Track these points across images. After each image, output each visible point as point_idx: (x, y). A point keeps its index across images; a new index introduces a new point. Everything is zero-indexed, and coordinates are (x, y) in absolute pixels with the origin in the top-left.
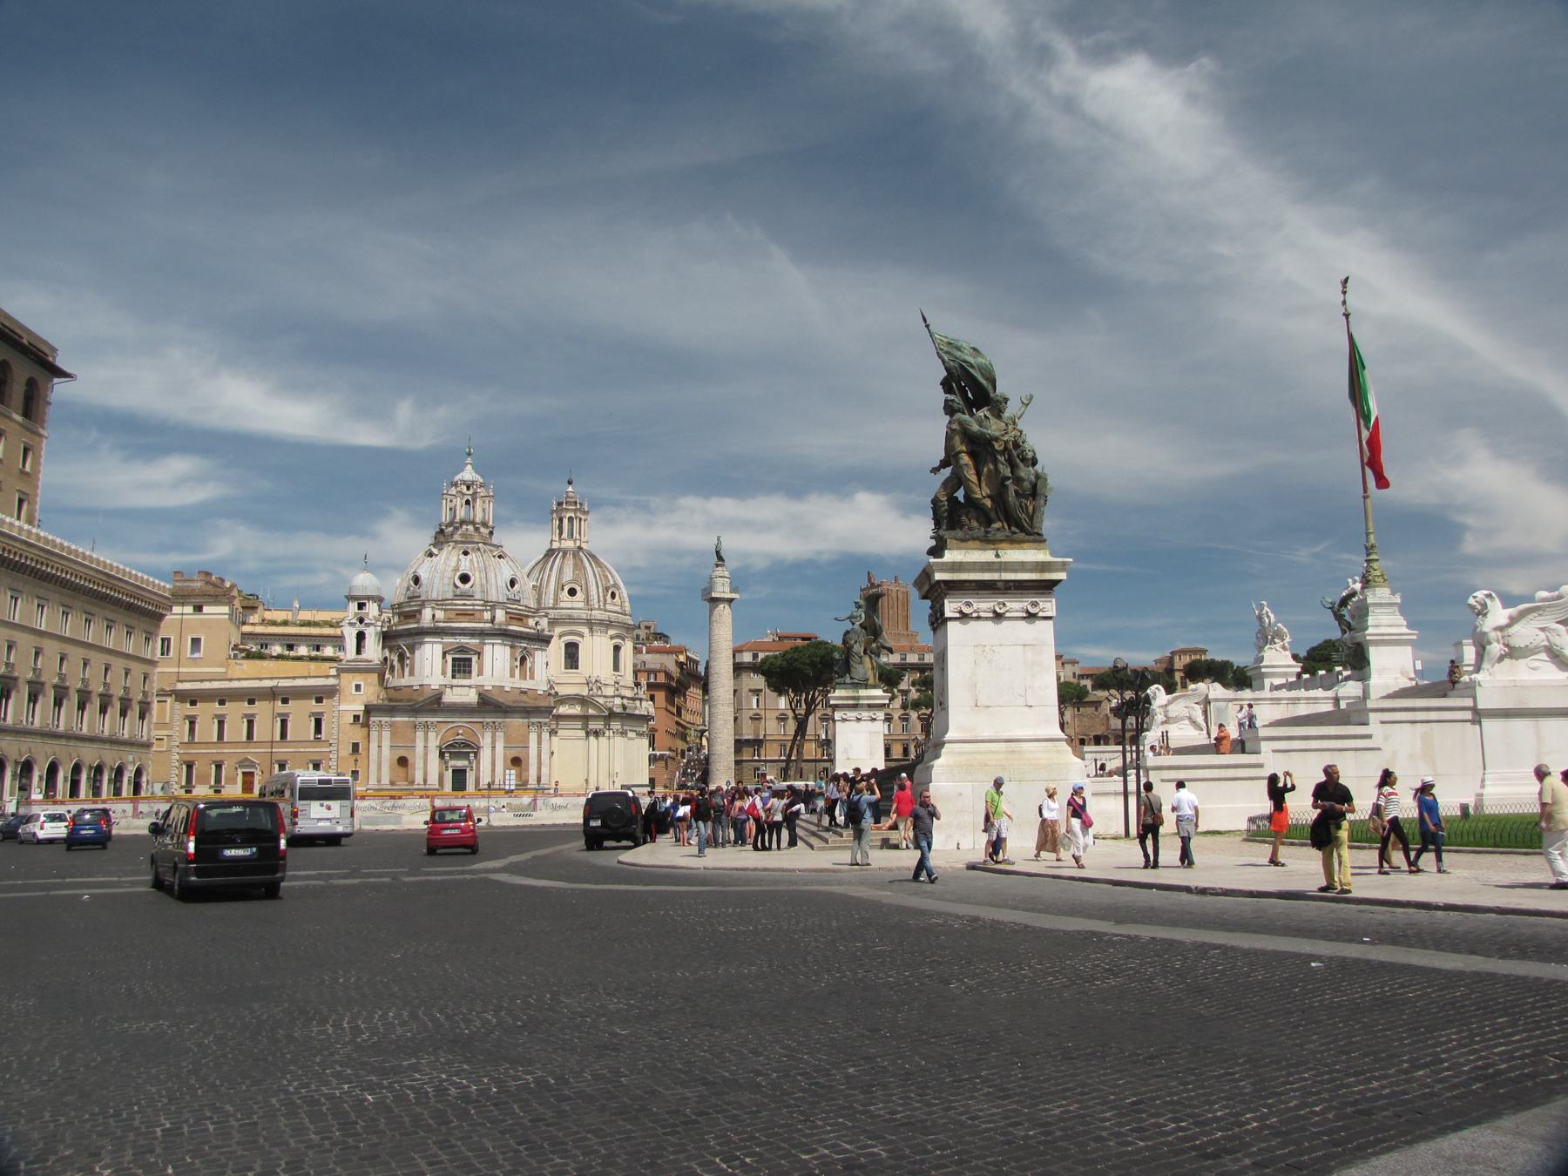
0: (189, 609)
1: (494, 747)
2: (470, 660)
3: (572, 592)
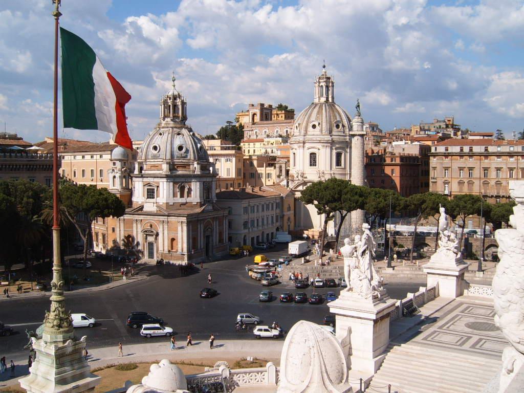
0: (99, 156)
1: (163, 233)
2: (154, 189)
3: (314, 126)
